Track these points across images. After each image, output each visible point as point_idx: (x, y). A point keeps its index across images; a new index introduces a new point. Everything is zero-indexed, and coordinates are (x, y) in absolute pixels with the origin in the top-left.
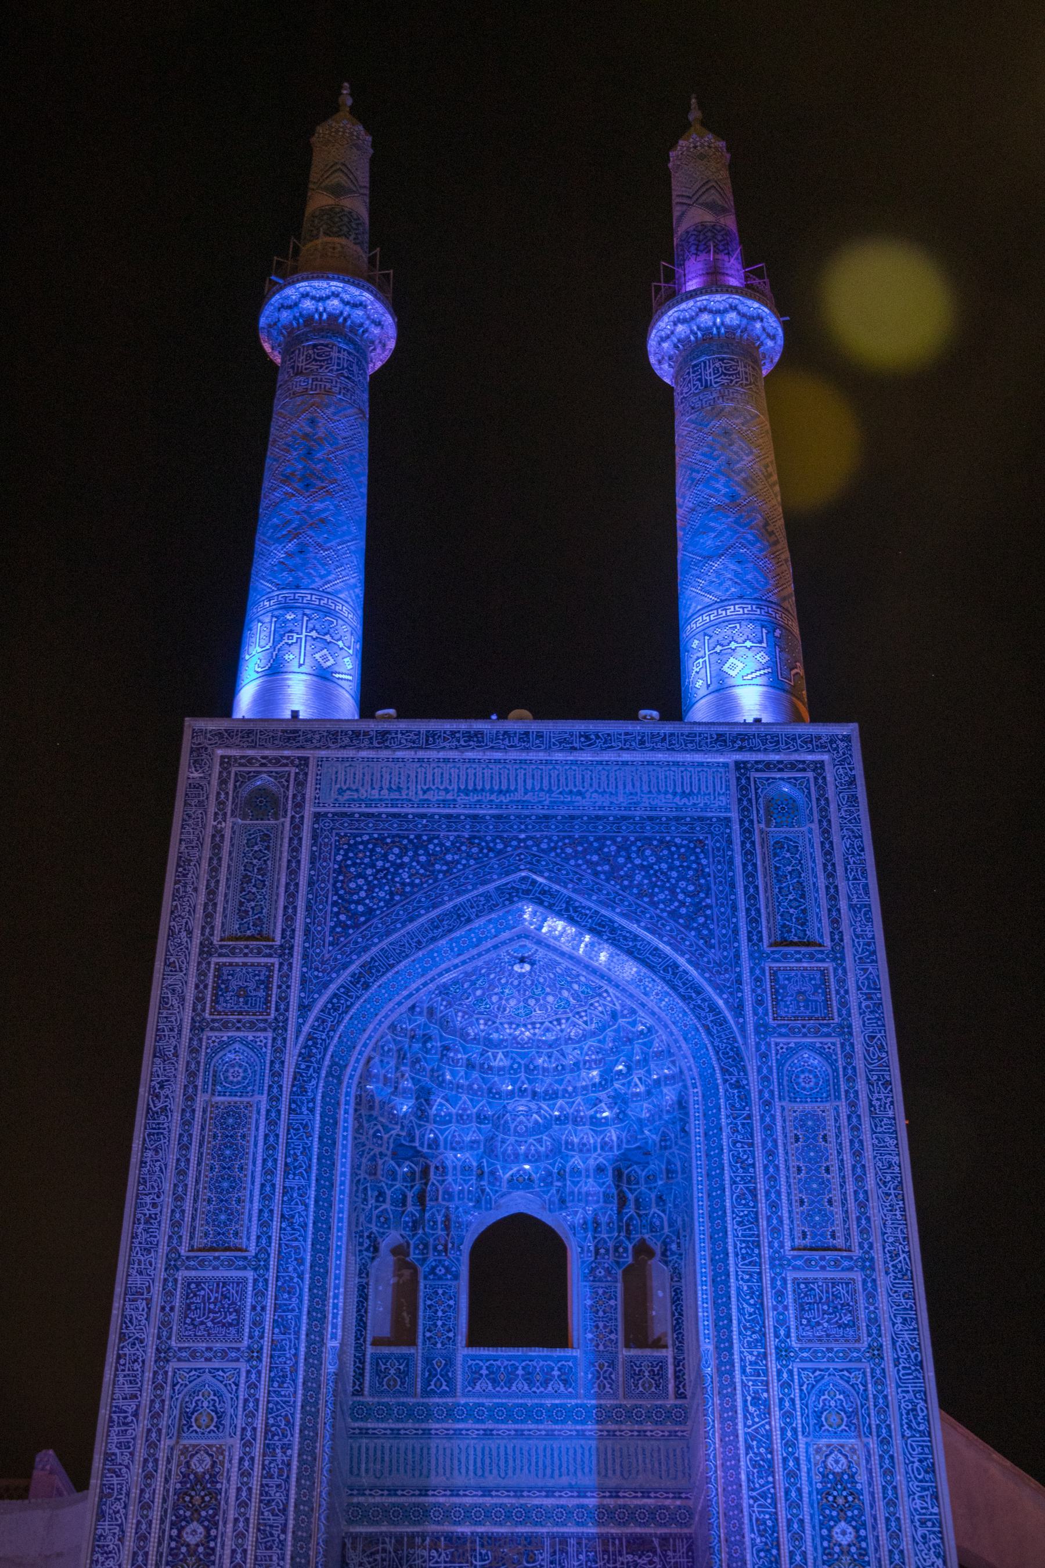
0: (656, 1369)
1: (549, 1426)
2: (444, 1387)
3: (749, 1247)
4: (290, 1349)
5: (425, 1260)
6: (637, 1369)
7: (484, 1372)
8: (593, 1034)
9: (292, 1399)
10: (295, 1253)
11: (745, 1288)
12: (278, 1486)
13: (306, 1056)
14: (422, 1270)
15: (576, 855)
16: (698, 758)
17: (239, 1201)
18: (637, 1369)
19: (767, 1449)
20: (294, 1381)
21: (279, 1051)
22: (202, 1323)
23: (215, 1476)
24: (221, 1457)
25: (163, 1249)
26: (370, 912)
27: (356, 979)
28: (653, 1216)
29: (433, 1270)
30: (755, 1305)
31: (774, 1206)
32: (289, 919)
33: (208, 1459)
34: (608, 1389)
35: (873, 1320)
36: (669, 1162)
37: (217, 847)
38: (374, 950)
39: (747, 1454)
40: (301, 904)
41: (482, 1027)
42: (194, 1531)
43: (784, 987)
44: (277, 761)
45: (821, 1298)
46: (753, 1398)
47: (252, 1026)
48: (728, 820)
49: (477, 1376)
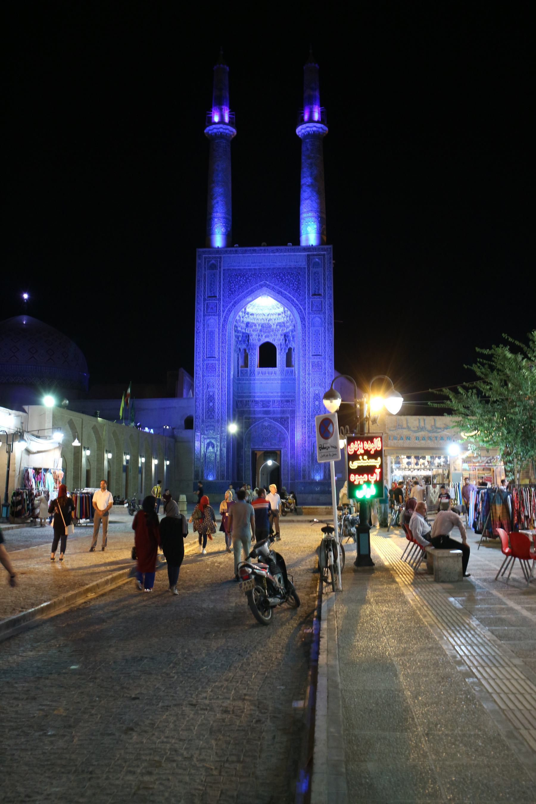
13: (224, 321)
15: (275, 277)
16: (300, 253)
21: (219, 320)
25: (202, 358)
26: (235, 291)
27: (233, 305)
31: (309, 348)
32: (220, 293)
35: (325, 368)
37: (205, 277)
38: (236, 299)
40: (222, 289)
44: (215, 257)
47: (214, 315)
48: (305, 268)
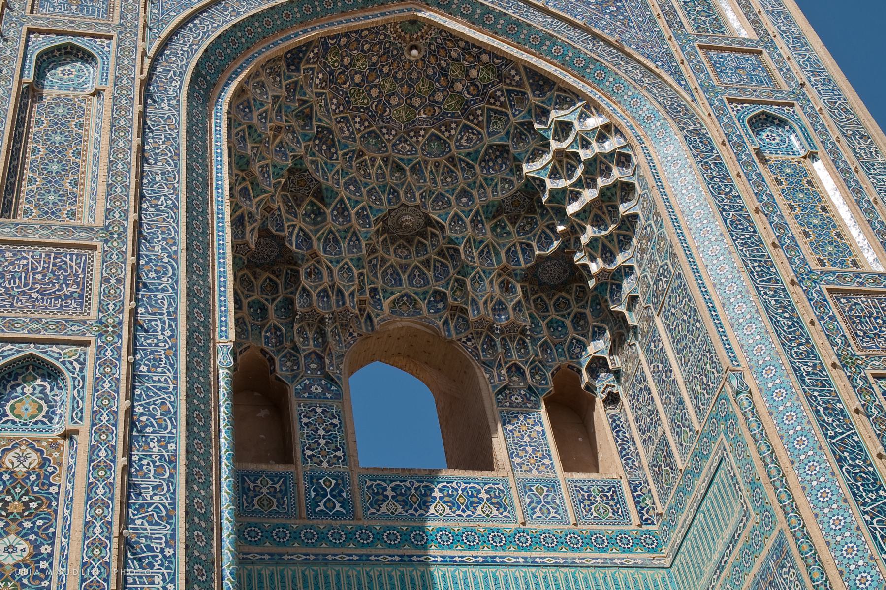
0: (609, 494)
1: (488, 552)
2: (338, 508)
3: (764, 266)
4: (163, 329)
5: (295, 376)
6: (586, 494)
7: (389, 493)
8: (490, 134)
9: (172, 386)
10: (163, 232)
11: (773, 302)
12: (155, 488)
14: (294, 388)
17: (75, 183)
18: (586, 494)
19: (864, 461)
20: (172, 366)
22: (24, 293)
23: (47, 477)
24: (56, 454)
28: (571, 342)
29: (306, 388)
30: (791, 318)
33: (34, 459)
34: (552, 515)
36: (604, 246)
39: (841, 467)
41: (358, 126)
42: (11, 546)
43: (722, 64)
45: (871, 314)
46: (825, 409)
49: (381, 497)
